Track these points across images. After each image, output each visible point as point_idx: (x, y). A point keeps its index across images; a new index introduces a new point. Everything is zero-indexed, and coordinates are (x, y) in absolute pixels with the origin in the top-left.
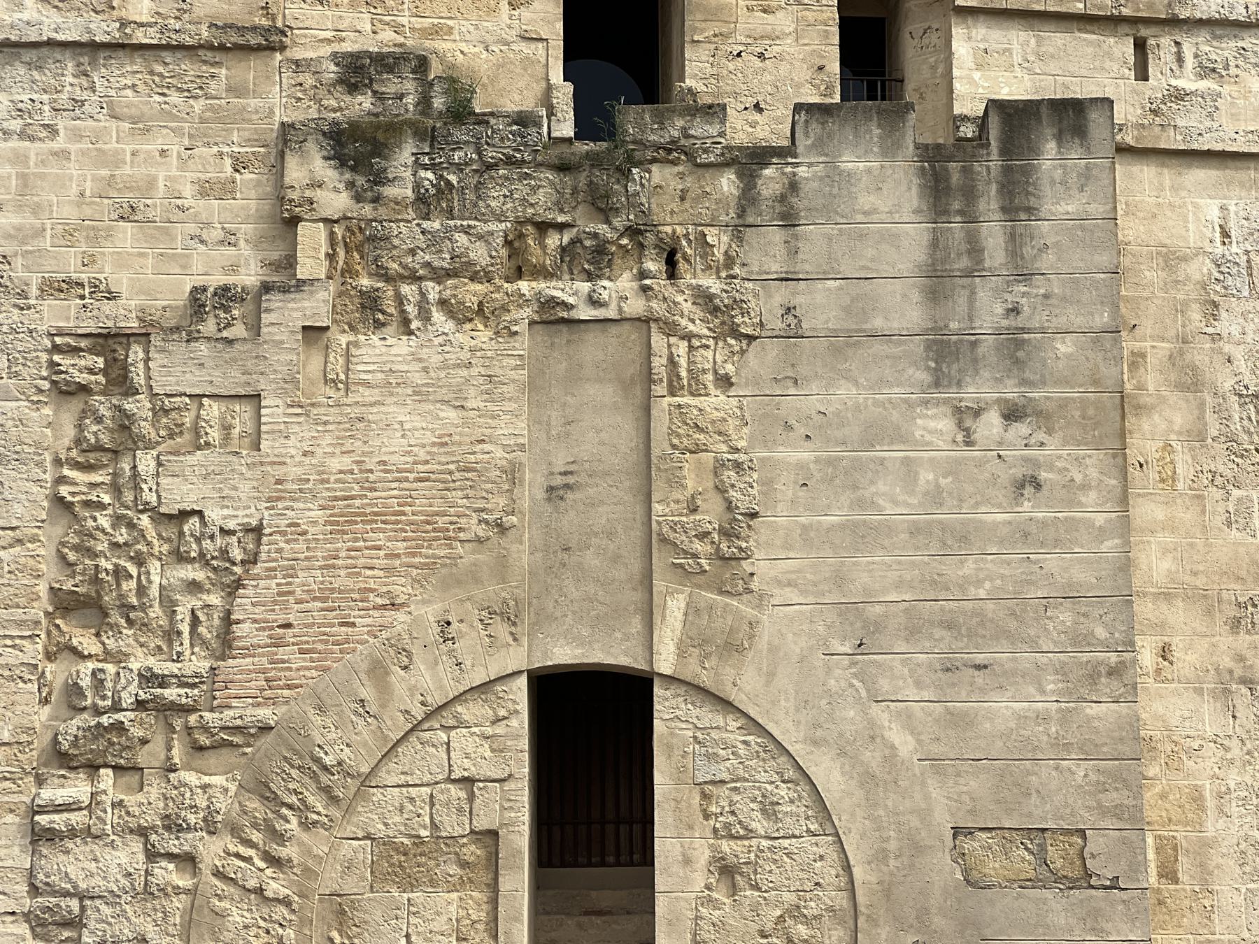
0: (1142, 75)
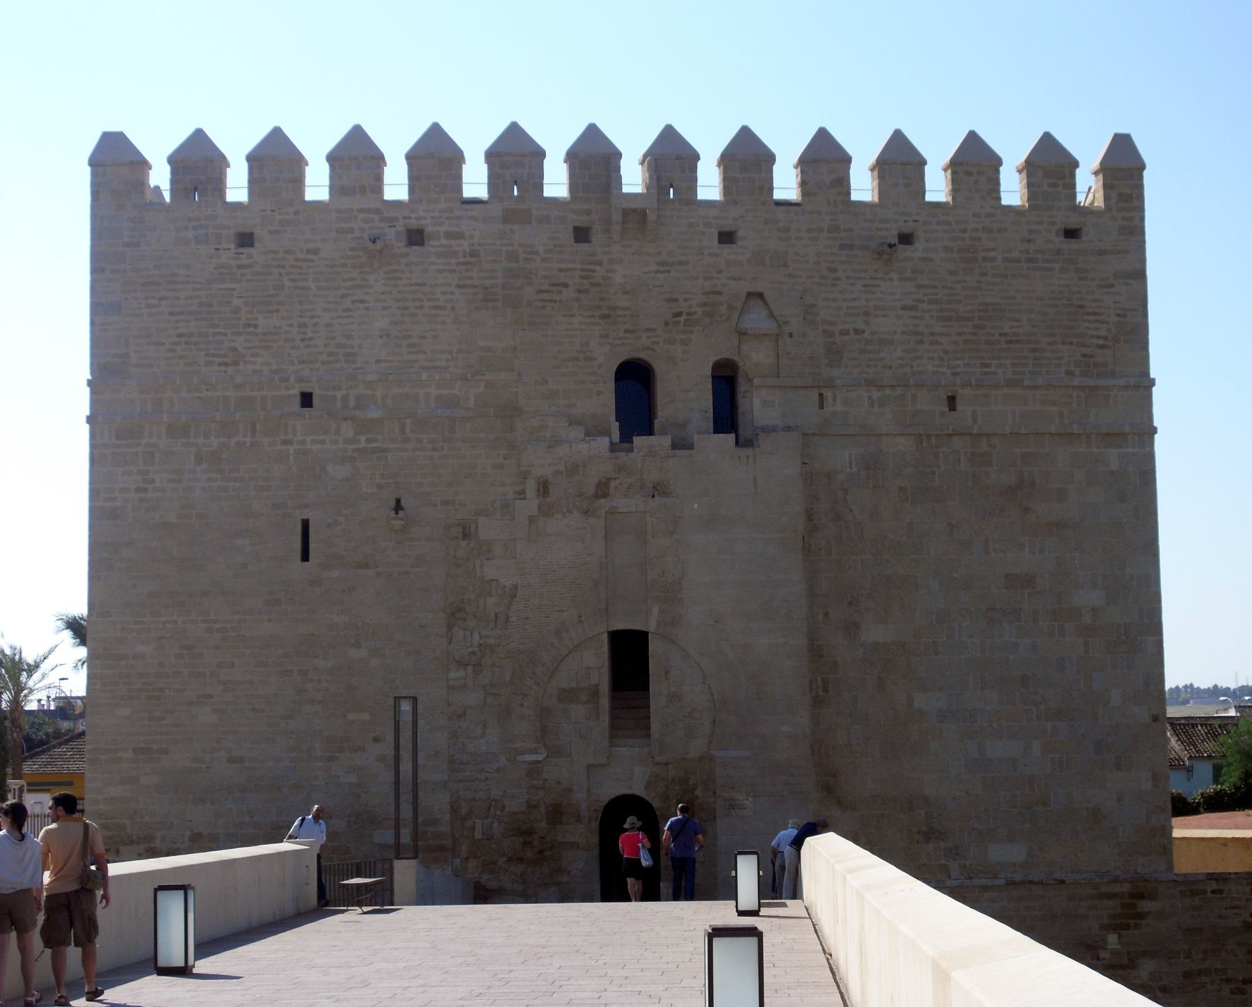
0: (821, 407)
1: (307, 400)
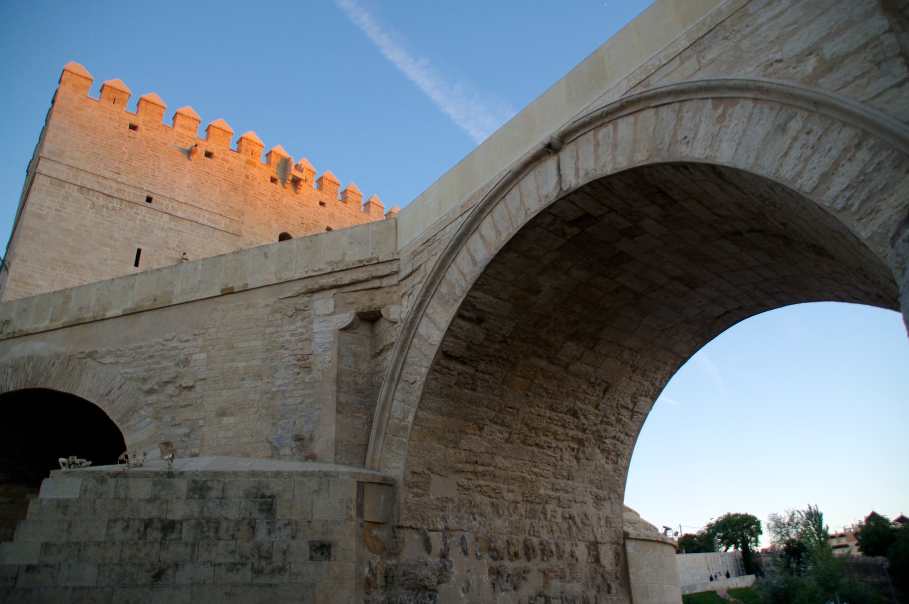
1: (149, 200)
